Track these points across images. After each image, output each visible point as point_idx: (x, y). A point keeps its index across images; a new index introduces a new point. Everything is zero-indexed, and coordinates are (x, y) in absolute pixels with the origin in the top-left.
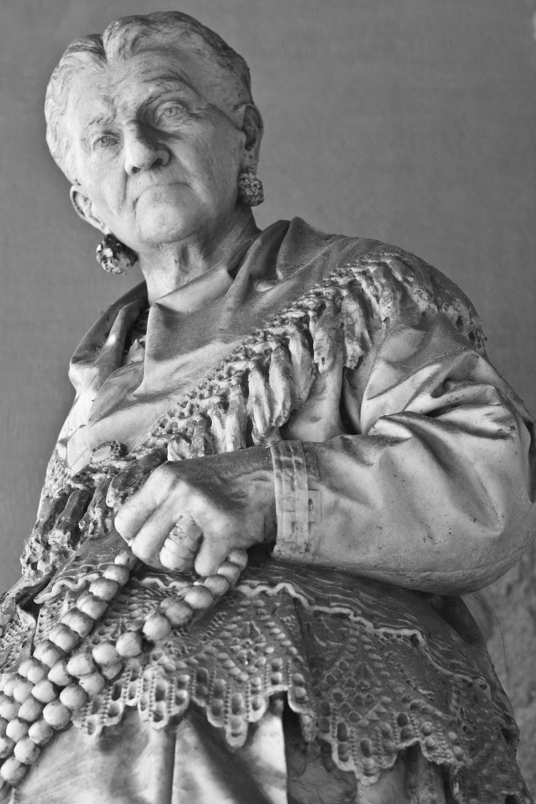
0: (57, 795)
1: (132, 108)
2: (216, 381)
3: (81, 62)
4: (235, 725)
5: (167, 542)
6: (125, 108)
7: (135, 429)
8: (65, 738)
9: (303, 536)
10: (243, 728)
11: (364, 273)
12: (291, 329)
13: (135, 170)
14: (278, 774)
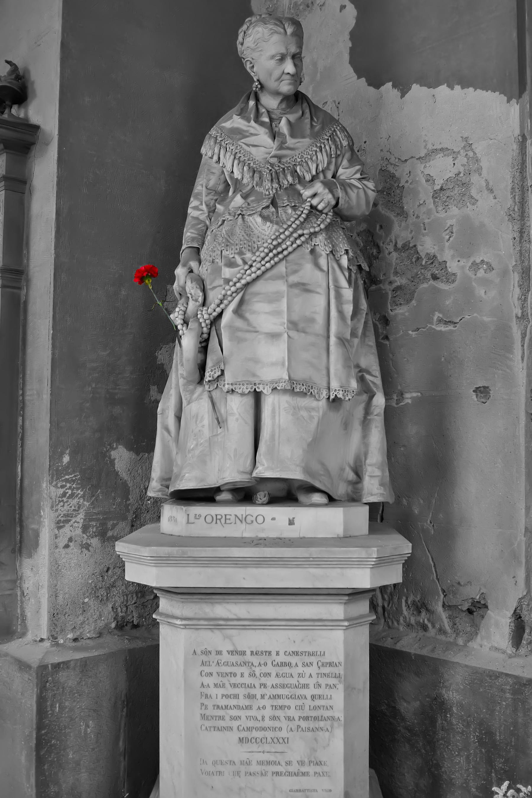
1: (292, 54)
8: (299, 248)
9: (343, 207)
10: (339, 256)
12: (326, 142)
13: (289, 73)
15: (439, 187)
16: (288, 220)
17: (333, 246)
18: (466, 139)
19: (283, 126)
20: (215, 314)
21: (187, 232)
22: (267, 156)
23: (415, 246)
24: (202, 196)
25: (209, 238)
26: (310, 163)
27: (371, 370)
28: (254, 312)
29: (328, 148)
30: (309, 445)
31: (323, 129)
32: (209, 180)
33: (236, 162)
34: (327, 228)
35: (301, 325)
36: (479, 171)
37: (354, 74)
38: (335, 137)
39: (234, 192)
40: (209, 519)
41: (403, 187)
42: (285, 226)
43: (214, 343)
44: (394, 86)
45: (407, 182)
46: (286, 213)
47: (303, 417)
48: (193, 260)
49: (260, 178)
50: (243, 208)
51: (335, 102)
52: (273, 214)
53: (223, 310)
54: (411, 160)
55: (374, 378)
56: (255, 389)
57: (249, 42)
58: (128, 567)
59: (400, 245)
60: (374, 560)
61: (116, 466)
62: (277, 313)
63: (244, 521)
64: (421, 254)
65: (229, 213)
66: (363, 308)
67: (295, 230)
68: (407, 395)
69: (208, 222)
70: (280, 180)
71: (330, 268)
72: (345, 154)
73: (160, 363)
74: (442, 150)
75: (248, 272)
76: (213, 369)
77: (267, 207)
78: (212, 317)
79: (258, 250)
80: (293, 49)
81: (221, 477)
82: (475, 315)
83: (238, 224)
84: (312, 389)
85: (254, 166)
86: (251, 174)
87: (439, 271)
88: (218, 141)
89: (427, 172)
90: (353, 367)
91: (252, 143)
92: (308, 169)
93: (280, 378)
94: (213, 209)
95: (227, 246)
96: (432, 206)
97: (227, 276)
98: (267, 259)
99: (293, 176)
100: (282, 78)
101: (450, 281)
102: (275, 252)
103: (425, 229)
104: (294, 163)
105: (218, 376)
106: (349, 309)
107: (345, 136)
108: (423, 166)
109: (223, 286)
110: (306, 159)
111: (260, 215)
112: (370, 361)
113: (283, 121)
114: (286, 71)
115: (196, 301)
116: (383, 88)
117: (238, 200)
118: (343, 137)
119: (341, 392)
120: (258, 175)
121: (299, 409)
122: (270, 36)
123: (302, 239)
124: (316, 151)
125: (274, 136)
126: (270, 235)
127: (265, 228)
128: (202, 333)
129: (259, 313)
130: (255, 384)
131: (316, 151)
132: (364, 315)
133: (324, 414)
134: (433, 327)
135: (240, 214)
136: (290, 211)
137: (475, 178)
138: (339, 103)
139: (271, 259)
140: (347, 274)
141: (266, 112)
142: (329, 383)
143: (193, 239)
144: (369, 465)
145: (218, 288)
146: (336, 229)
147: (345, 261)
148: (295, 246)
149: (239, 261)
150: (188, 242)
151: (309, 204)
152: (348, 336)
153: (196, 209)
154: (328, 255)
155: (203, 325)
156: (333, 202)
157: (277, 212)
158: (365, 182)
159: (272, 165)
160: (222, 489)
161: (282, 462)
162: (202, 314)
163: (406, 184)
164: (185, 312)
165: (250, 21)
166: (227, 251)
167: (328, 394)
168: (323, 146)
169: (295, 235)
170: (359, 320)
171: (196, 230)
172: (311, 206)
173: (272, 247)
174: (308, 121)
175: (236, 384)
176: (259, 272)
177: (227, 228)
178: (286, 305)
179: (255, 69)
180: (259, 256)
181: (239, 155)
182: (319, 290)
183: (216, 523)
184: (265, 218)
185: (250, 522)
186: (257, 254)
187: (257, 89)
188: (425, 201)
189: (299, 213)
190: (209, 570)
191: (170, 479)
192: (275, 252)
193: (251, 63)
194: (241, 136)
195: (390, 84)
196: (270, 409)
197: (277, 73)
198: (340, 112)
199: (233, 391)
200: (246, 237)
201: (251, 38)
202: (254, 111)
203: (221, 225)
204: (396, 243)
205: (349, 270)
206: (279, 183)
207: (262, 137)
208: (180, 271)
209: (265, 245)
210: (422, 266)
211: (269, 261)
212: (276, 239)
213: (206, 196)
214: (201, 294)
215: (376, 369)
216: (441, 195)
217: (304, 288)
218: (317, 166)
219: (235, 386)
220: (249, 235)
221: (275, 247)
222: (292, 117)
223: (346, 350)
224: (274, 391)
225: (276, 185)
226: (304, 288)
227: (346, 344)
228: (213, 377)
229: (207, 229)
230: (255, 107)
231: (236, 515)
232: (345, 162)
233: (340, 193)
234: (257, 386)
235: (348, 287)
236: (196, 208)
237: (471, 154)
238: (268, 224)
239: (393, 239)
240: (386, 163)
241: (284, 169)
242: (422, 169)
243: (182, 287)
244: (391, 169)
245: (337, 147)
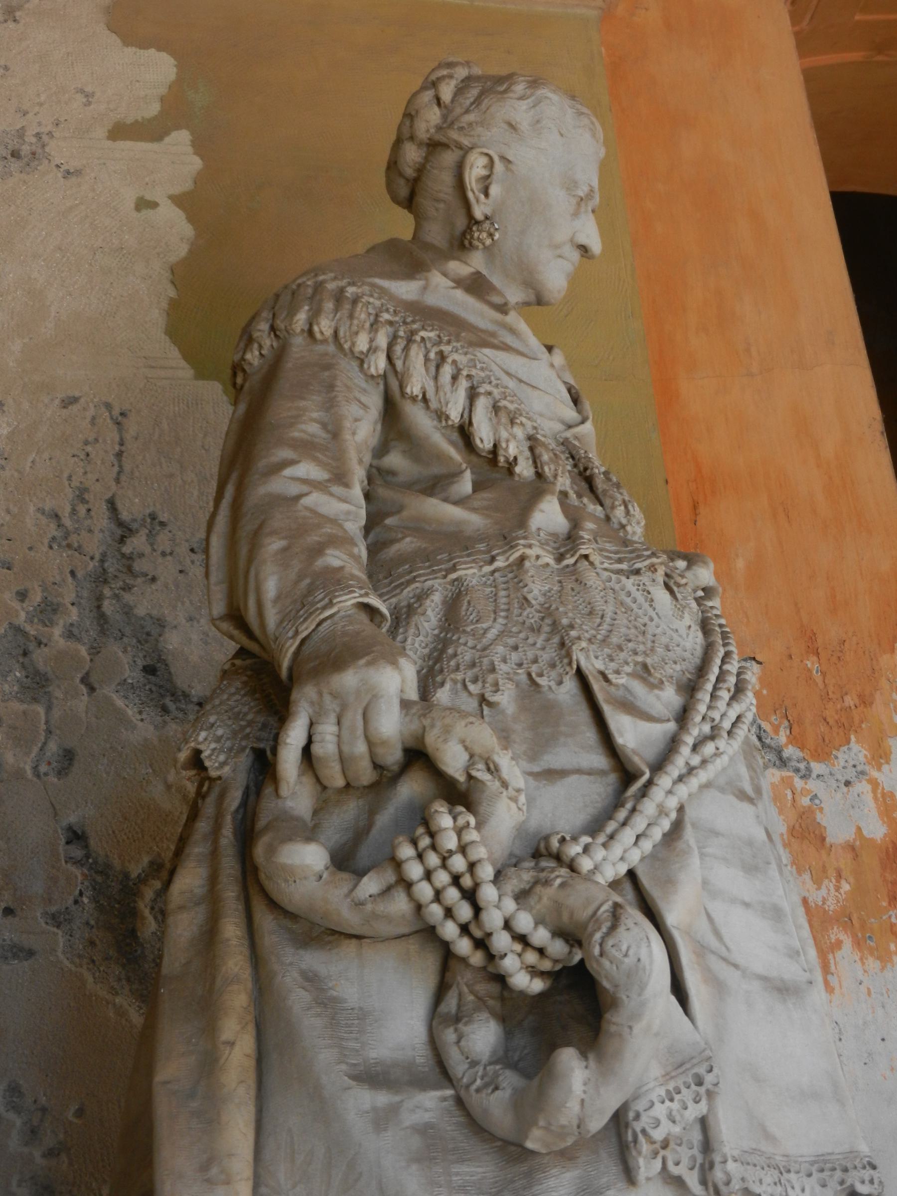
114: (582, 239)
145: (574, 778)
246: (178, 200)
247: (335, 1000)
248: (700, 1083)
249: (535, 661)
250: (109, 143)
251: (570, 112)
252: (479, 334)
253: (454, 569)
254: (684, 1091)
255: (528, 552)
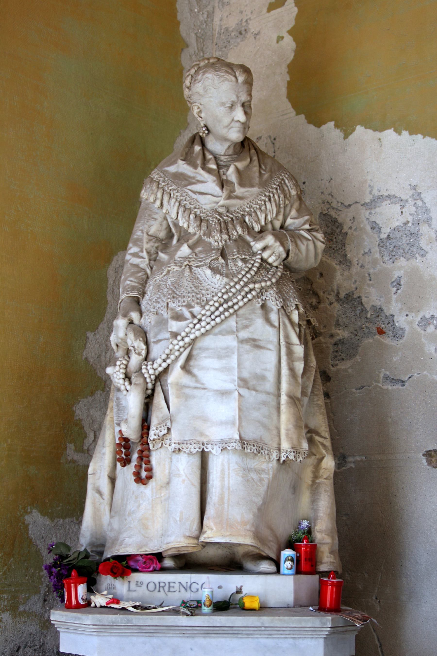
0: (250, 317)
1: (242, 102)
2: (257, 200)
3: (232, 80)
4: (288, 310)
5: (272, 257)
6: (241, 101)
7: (234, 205)
8: (250, 303)
10: (290, 311)
11: (285, 176)
12: (275, 191)
13: (239, 121)
14: (296, 324)
15: (385, 236)
16: (239, 273)
17: (284, 300)
18: (415, 188)
19: (231, 174)
20: (160, 369)
21: (126, 279)
22: (214, 205)
23: (359, 297)
24: (143, 243)
25: (150, 288)
26: (259, 213)
27: (319, 431)
28: (203, 368)
29: (276, 197)
30: (259, 509)
31: (271, 177)
32: (150, 226)
33: (181, 209)
34: (277, 282)
35: (252, 383)
36: (428, 221)
37: (292, 110)
38: (284, 186)
39: (178, 240)
40: (151, 586)
41: (346, 233)
42: (236, 280)
43: (159, 398)
44: (336, 126)
45: (351, 228)
46: (236, 265)
47: (253, 479)
48: (133, 310)
49: (207, 228)
50: (190, 258)
51: (270, 137)
52: (222, 266)
53: (169, 365)
54: (355, 205)
55: (323, 439)
56: (203, 449)
57: (198, 87)
58: (63, 636)
59: (342, 295)
60: (329, 629)
61: (30, 532)
62: (227, 370)
63: (188, 589)
64: (366, 306)
65: (175, 263)
66: (312, 365)
67: (246, 284)
68: (350, 459)
69: (149, 271)
70: (230, 230)
71: (281, 324)
72: (293, 203)
73: (77, 418)
74: (389, 197)
75: (198, 326)
76: (158, 427)
77: (217, 259)
78: (157, 373)
79: (207, 303)
80: (244, 98)
81: (165, 542)
82: (425, 373)
83: (185, 275)
84: (262, 449)
85: (201, 215)
86: (198, 223)
87: (386, 324)
88: (160, 186)
89: (373, 219)
90: (303, 427)
91: (198, 191)
92: (256, 219)
93: (231, 437)
94: (154, 256)
95: (174, 297)
96: (377, 255)
97: (174, 329)
98: (217, 313)
99: (242, 227)
100: (231, 125)
101: (397, 336)
102: (225, 306)
103: (370, 280)
104: (242, 213)
105: (164, 435)
106: (300, 366)
107: (294, 185)
108: (368, 212)
109: (171, 340)
110: (255, 209)
111: (210, 267)
112: (320, 422)
113: (232, 169)
114: (236, 119)
115: (139, 354)
116: (324, 127)
117: (185, 250)
118: (292, 186)
119: (292, 453)
120: (205, 225)
121: (249, 471)
122: (221, 83)
123: (254, 293)
124: (265, 201)
125: (222, 184)
126: (220, 288)
127: (215, 280)
128: (147, 389)
129: (208, 369)
130: (203, 444)
131: (265, 201)
132: (313, 373)
133: (275, 477)
134: (380, 385)
135: (188, 265)
136: (240, 263)
137: (424, 229)
138: (275, 139)
139: (222, 313)
140: (297, 330)
141: (213, 159)
142: (279, 444)
143: (133, 288)
144: (317, 531)
145: (163, 341)
146: (286, 282)
147: (295, 317)
148: (246, 300)
149: (187, 315)
150: (128, 291)
151: (259, 257)
152: (299, 395)
153: (135, 256)
154: (279, 310)
155: (148, 380)
156: (284, 256)
157: (227, 265)
158: (315, 233)
159: (220, 214)
160: (164, 555)
161: (229, 527)
162: (147, 369)
163: (350, 230)
164: (127, 366)
165: (198, 65)
166: (174, 303)
167: (278, 456)
168: (272, 195)
169: (247, 289)
170: (308, 378)
171: (136, 278)
172: (262, 259)
173: (222, 301)
174: (256, 169)
175: (183, 444)
176: (208, 327)
177: (173, 279)
178: (236, 361)
179: (203, 115)
180: (209, 310)
181: (185, 202)
182: (270, 346)
183: (159, 591)
184: (215, 270)
185: (196, 590)
186: (207, 307)
187: (204, 135)
188: (370, 250)
189: (250, 266)
190: (155, 641)
191: (103, 546)
192: (225, 306)
193: (199, 108)
194: (186, 182)
195: (332, 124)
196: (219, 469)
197: (226, 121)
198: (276, 149)
199: (179, 450)
200: (193, 289)
201: (200, 84)
202: (201, 157)
203: (166, 275)
204: (338, 293)
205: (300, 326)
206: (228, 234)
207: (210, 185)
208: (120, 323)
209: (215, 299)
210: (367, 318)
211: (219, 316)
212: (227, 292)
213: (147, 243)
214: (144, 347)
215: (324, 430)
216: (388, 244)
217: (255, 344)
218: (266, 216)
219: (183, 445)
220: (197, 287)
221: (226, 301)
222: (241, 165)
223: (297, 409)
224: (223, 451)
225: (225, 237)
226: (255, 344)
227: (297, 402)
228: (158, 436)
229: (148, 278)
230: (201, 152)
231: (180, 583)
232: (294, 213)
233: (291, 247)
234: (206, 445)
235: (298, 343)
236: (135, 255)
237: (420, 203)
238: (218, 276)
239: (335, 287)
240: (328, 206)
241: (232, 219)
242: (367, 216)
243: (122, 339)
244: (332, 213)
245: (285, 196)
246: (290, 32)
247: (122, 404)
248: (166, 425)
249: (162, 306)
250: (268, 15)
251: (216, 78)
252: (190, 180)
253: (154, 278)
254: (163, 427)
255: (169, 269)
